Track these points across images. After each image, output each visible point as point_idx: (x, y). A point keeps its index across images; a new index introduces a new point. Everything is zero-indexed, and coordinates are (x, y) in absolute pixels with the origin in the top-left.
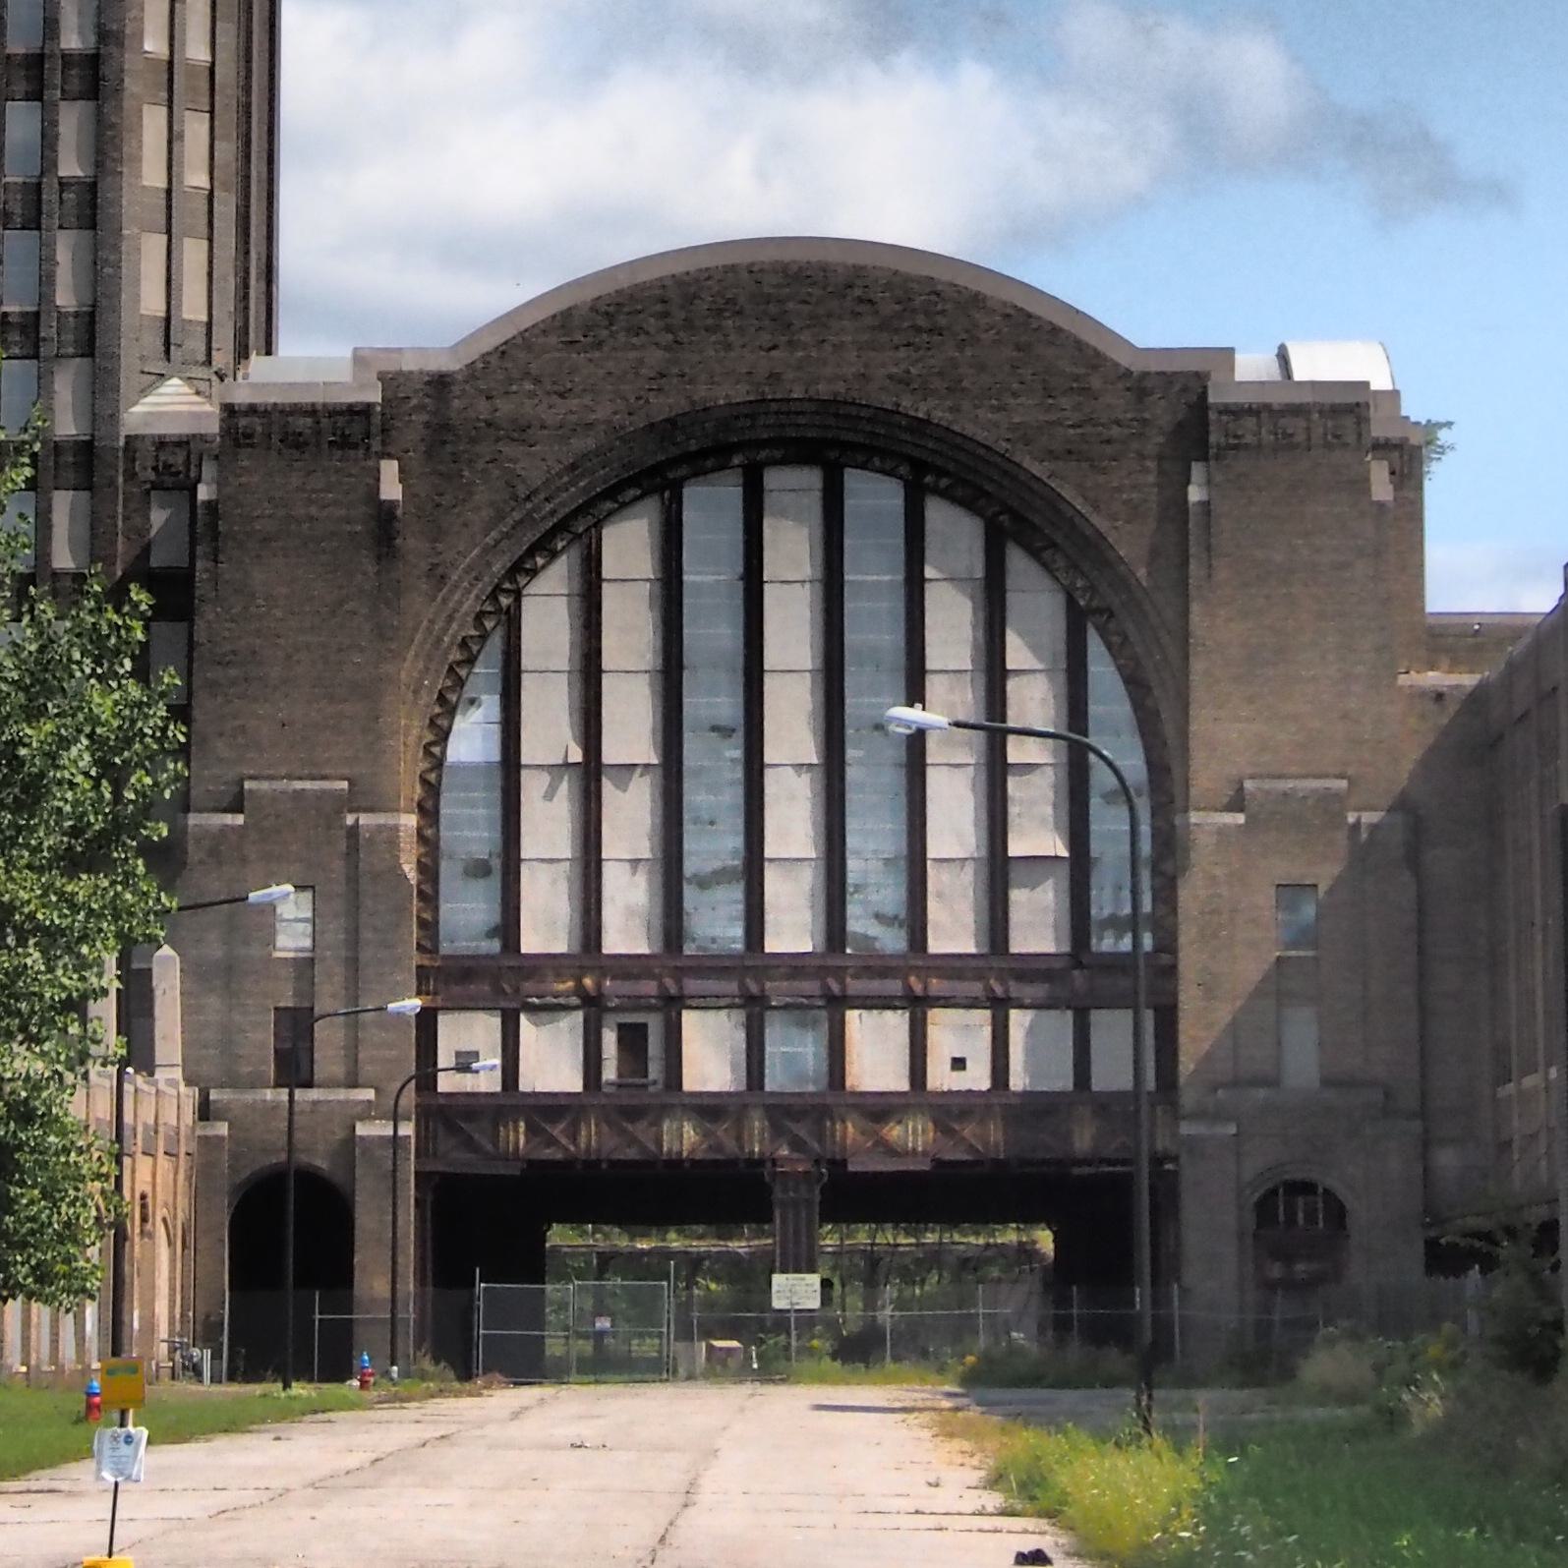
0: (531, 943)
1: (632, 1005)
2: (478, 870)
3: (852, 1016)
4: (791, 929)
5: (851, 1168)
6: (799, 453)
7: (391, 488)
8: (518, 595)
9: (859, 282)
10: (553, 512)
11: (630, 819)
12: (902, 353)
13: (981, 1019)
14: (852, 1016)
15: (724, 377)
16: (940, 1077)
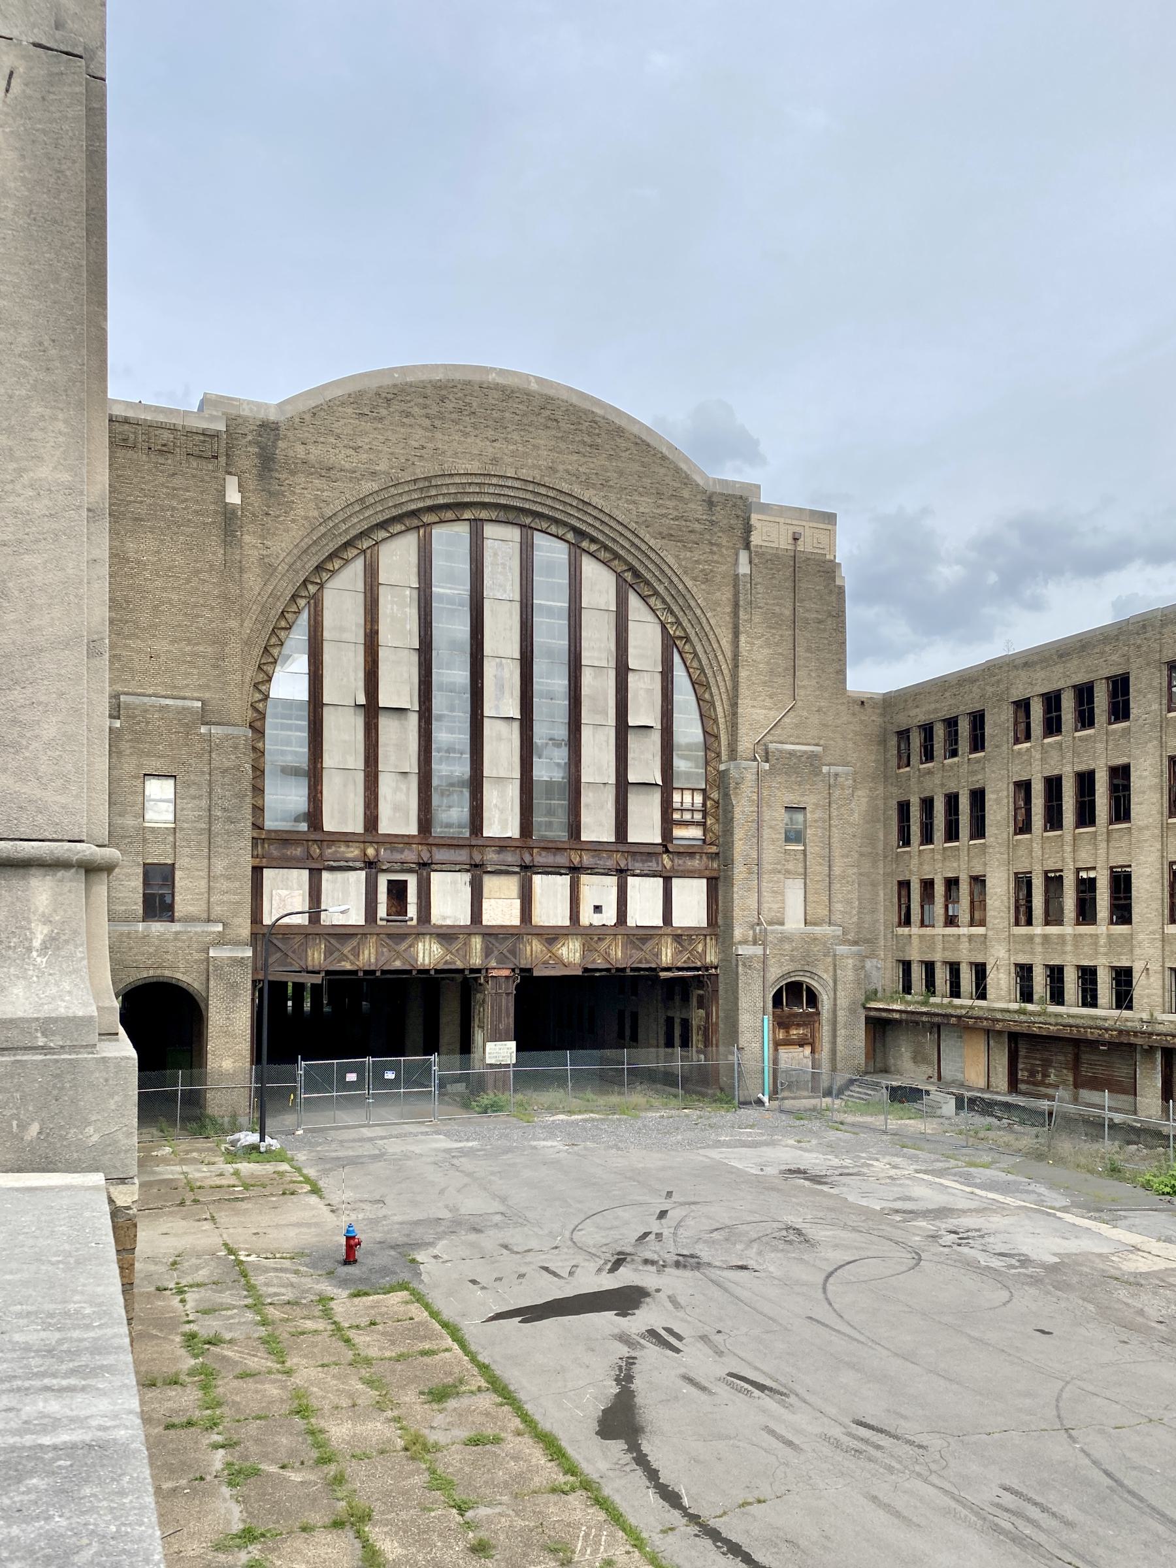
0: (330, 824)
1: (397, 869)
2: (290, 772)
3: (537, 879)
4: (502, 820)
5: (536, 974)
6: (509, 514)
7: (233, 497)
8: (321, 586)
9: (549, 407)
10: (346, 531)
11: (399, 742)
12: (575, 457)
13: (612, 881)
14: (537, 879)
15: (465, 455)
16: (587, 917)
